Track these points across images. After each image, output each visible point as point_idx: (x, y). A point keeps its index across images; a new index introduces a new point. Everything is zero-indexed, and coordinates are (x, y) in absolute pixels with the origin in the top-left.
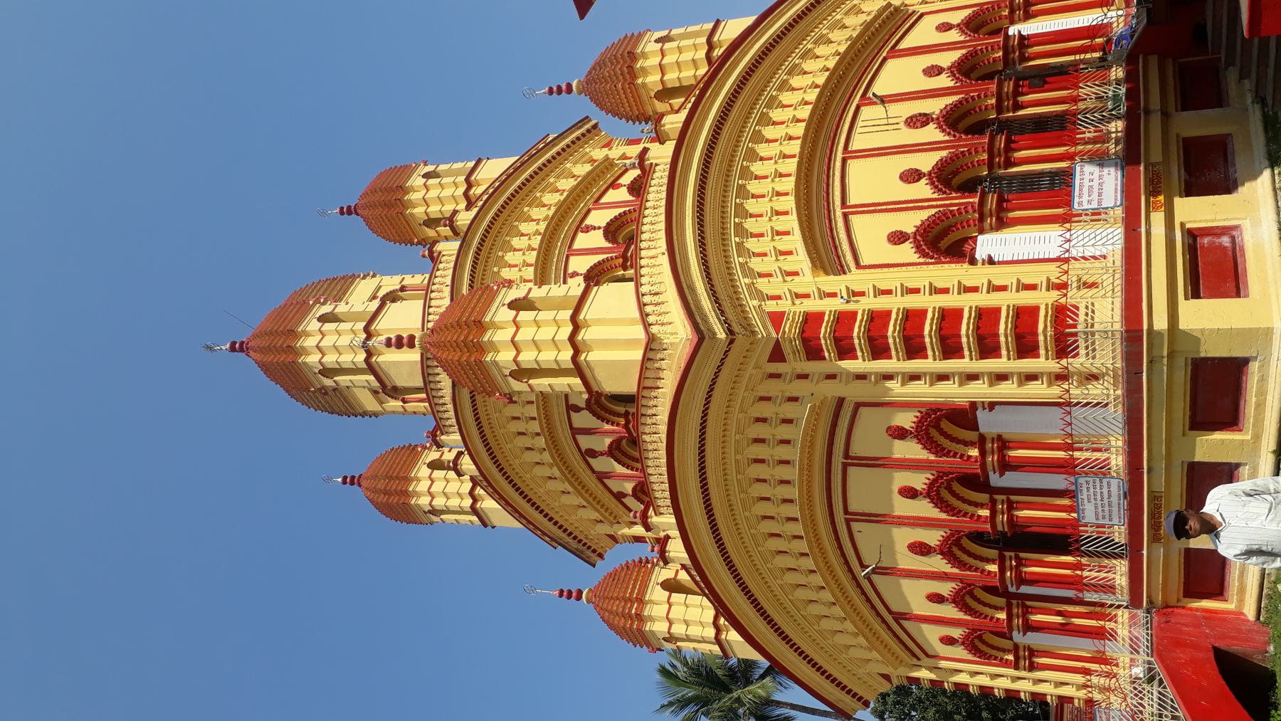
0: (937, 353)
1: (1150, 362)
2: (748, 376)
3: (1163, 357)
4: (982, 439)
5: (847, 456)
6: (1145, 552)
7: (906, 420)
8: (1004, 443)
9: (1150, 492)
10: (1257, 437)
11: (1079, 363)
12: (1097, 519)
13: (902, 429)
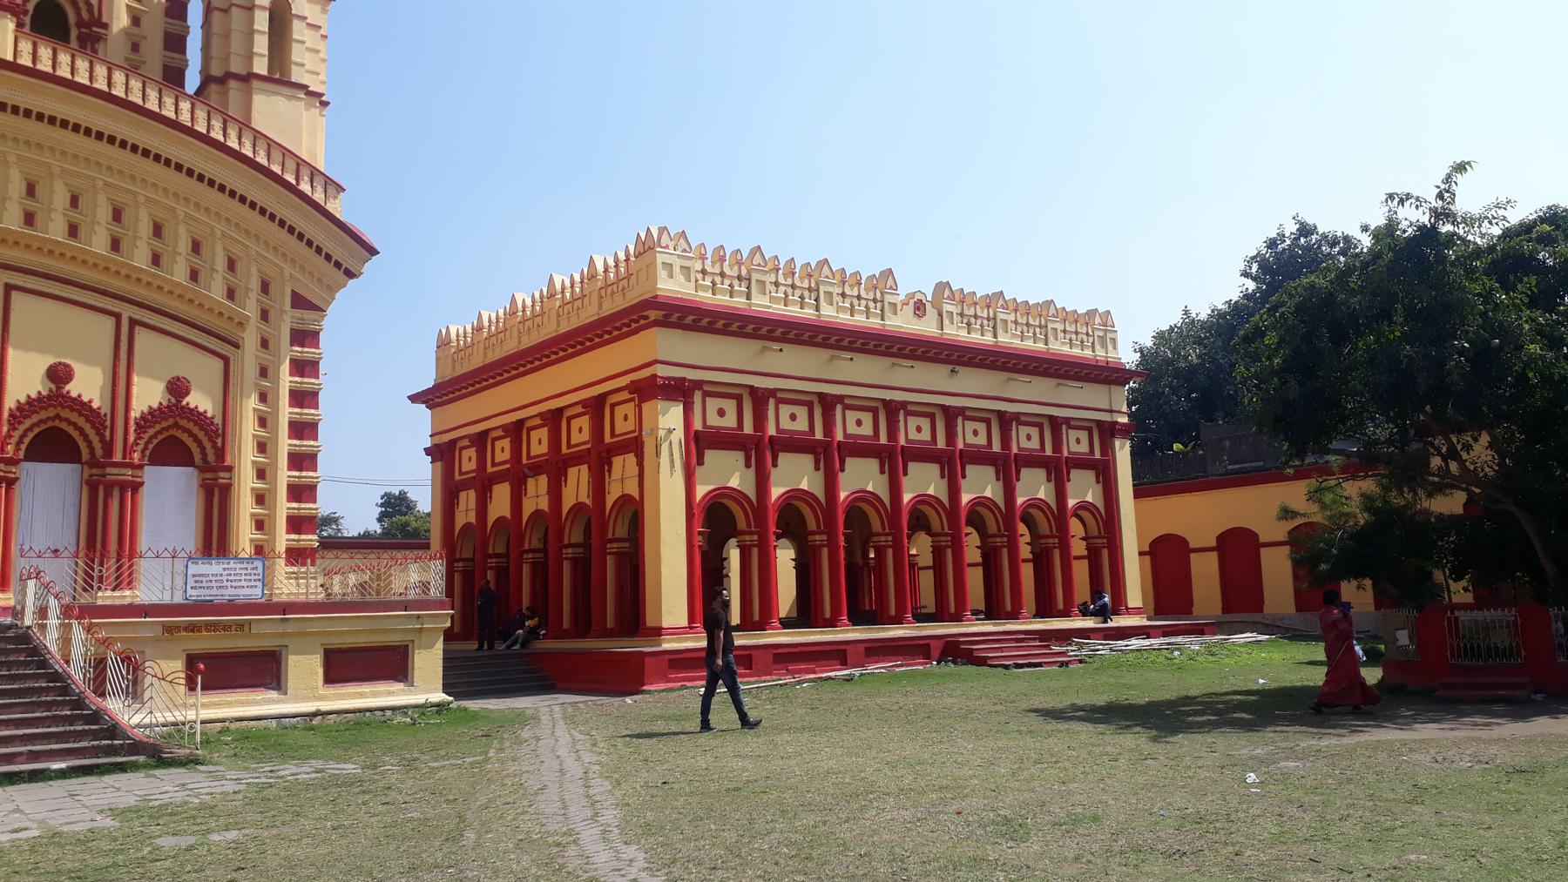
0: (297, 448)
1: (418, 617)
2: (284, 266)
3: (422, 624)
4: (140, 467)
5: (133, 323)
6: (143, 619)
7: (201, 400)
8: (136, 487)
9: (250, 622)
10: (322, 698)
11: (281, 567)
12: (194, 576)
13: (187, 393)
